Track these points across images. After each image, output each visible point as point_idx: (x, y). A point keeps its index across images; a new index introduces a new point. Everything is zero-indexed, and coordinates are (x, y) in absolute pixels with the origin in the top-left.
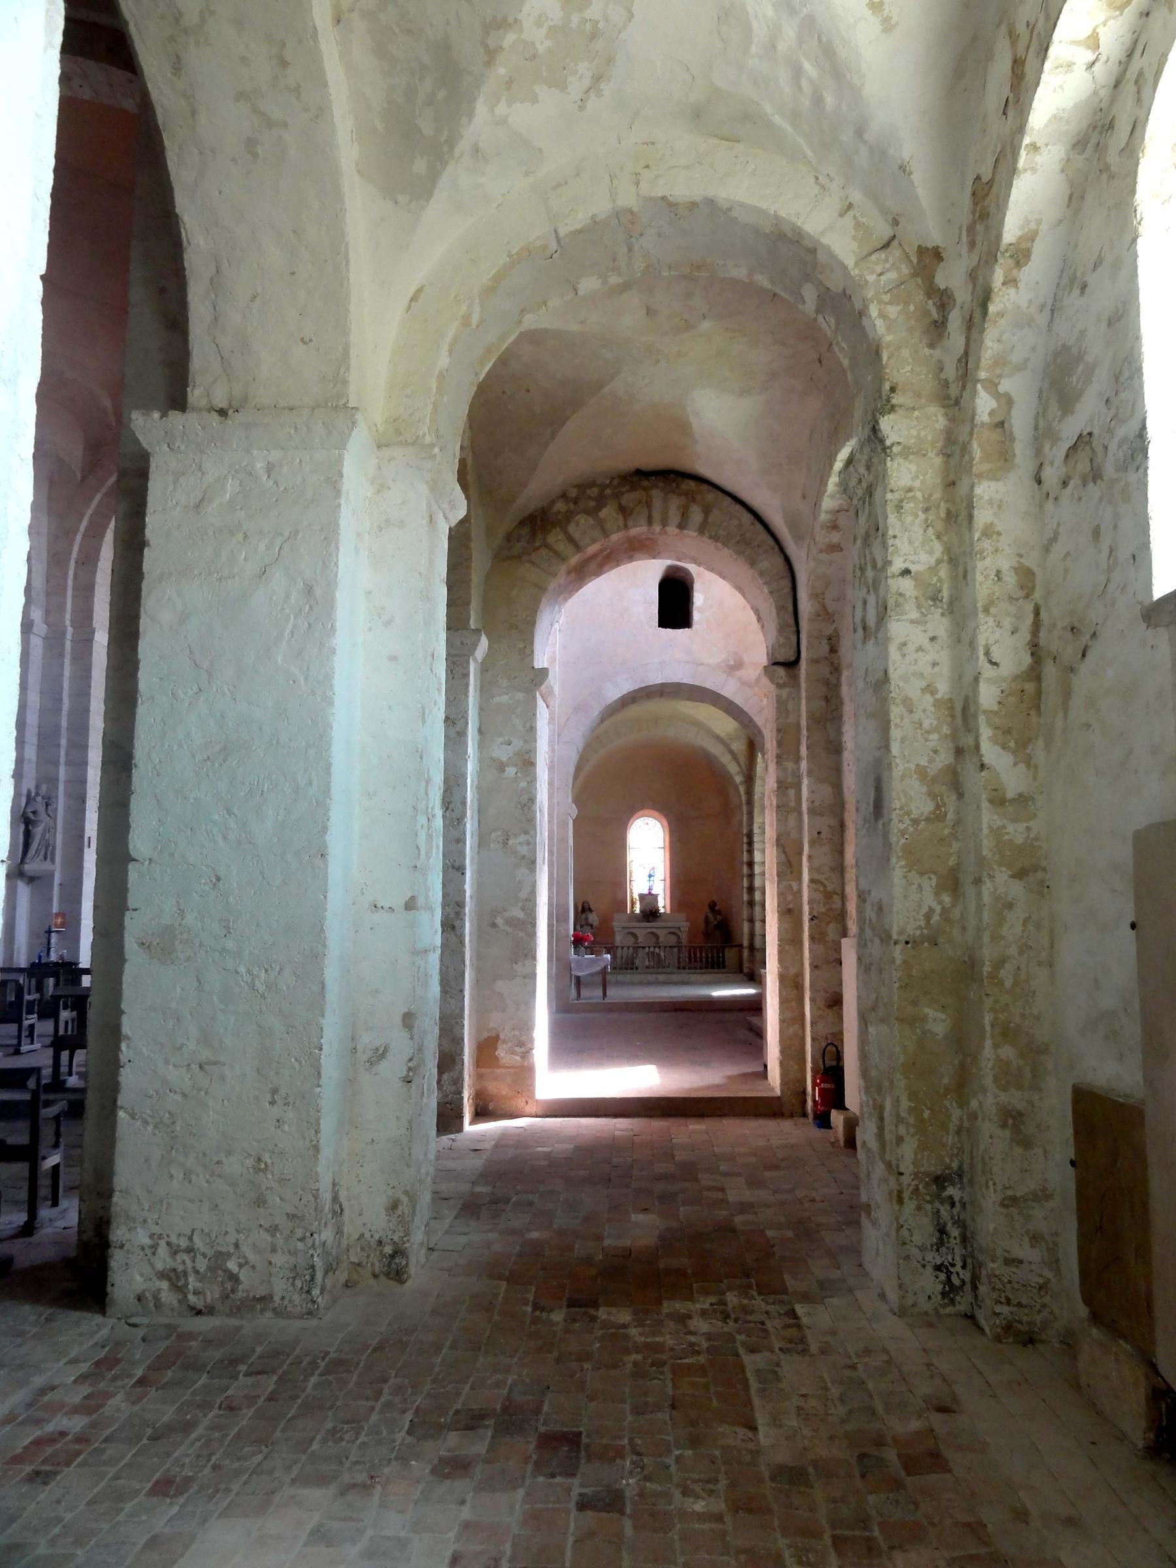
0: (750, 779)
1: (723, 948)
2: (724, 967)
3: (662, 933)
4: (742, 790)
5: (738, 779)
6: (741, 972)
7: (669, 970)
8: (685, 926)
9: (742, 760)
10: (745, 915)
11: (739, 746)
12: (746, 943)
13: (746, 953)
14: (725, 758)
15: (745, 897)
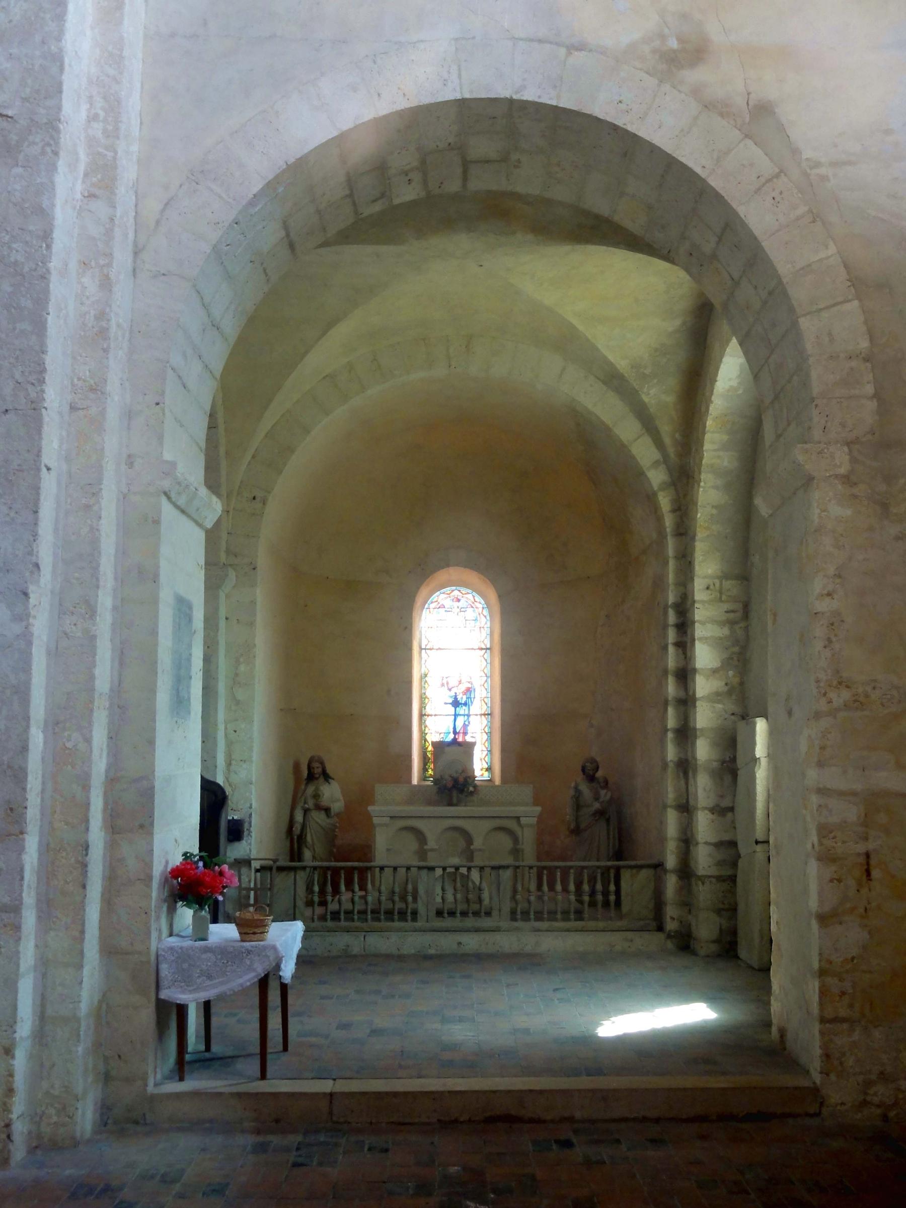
0: (684, 477)
1: (618, 870)
2: (621, 917)
3: (479, 831)
4: (665, 502)
5: (657, 477)
6: (660, 928)
7: (486, 922)
8: (530, 813)
9: (667, 430)
10: (671, 796)
11: (660, 395)
12: (671, 861)
13: (671, 883)
14: (627, 430)
15: (672, 753)
